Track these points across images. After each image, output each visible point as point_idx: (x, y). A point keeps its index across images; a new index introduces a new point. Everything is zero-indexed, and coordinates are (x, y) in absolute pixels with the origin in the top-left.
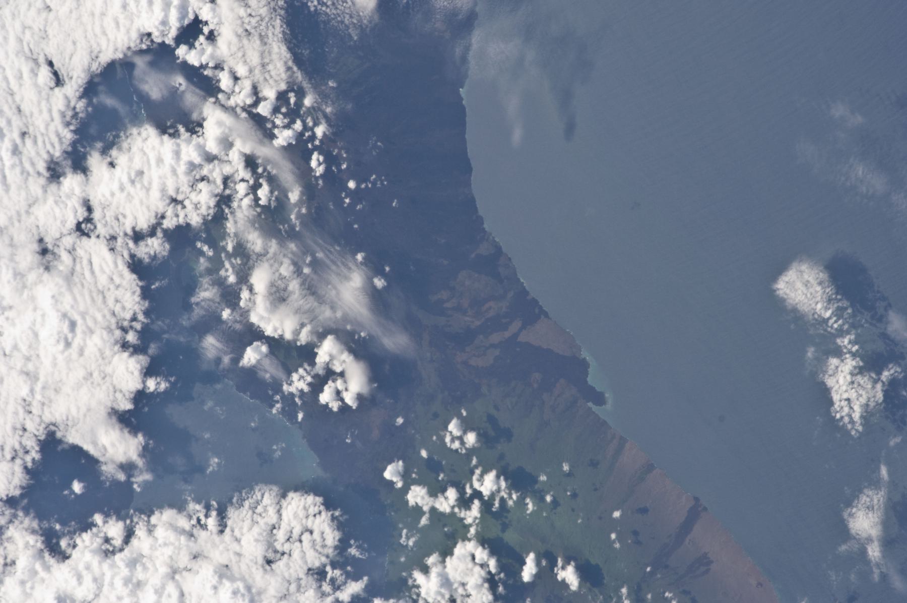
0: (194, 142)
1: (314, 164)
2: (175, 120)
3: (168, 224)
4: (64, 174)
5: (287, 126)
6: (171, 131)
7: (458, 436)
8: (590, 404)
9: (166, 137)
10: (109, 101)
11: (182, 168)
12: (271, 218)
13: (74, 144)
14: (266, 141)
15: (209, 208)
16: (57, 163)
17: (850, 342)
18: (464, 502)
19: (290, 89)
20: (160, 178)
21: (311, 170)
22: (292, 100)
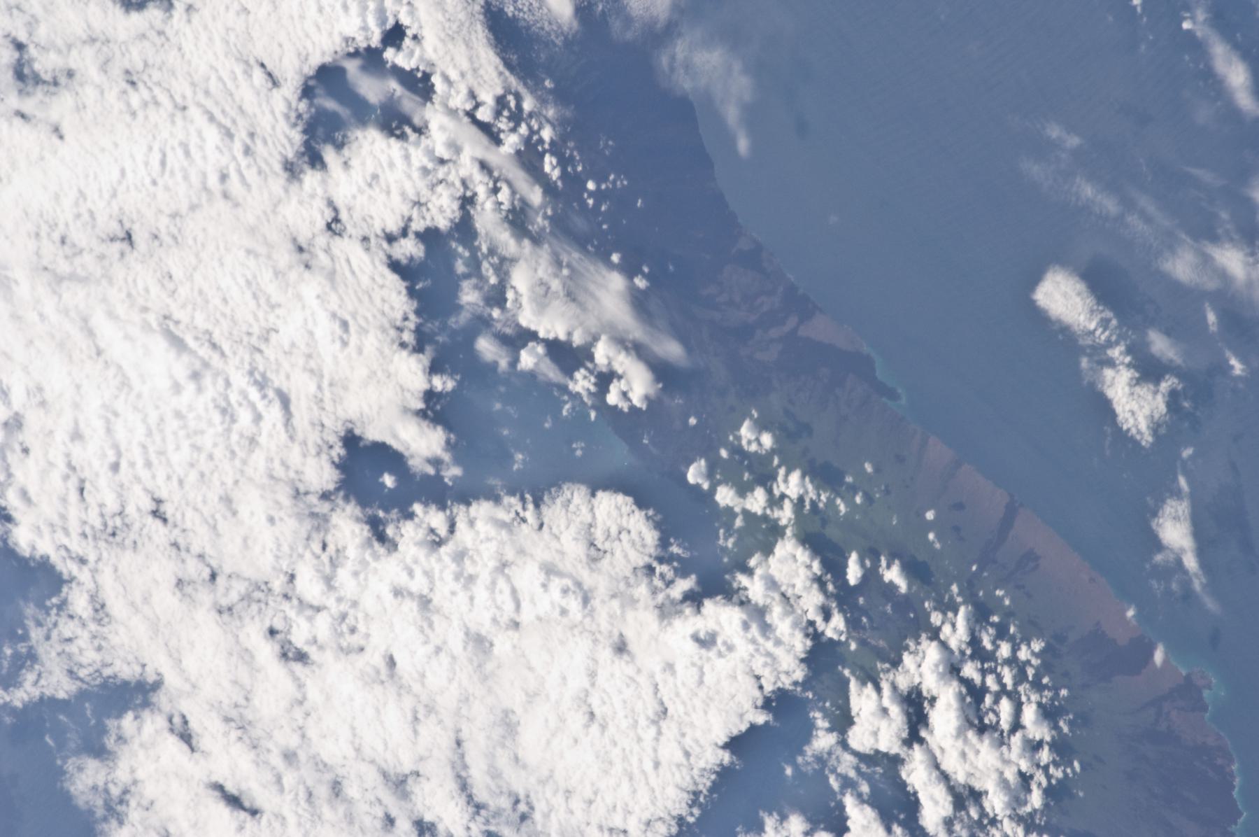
0: (423, 146)
1: (547, 168)
2: (395, 123)
3: (418, 225)
4: (302, 171)
5: (514, 130)
6: (398, 132)
7: (752, 437)
8: (884, 399)
9: (393, 140)
10: (330, 105)
11: (416, 175)
12: (518, 219)
13: (307, 144)
14: (493, 148)
15: (453, 212)
16: (292, 164)
17: (1121, 353)
18: (775, 501)
19: (508, 91)
20: (396, 182)
21: (546, 175)
22: (513, 104)
